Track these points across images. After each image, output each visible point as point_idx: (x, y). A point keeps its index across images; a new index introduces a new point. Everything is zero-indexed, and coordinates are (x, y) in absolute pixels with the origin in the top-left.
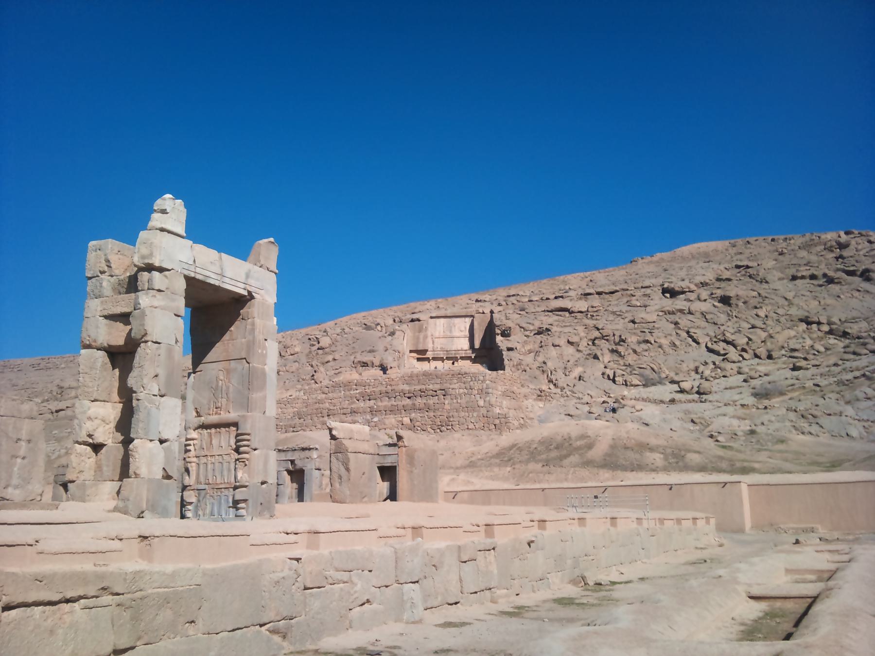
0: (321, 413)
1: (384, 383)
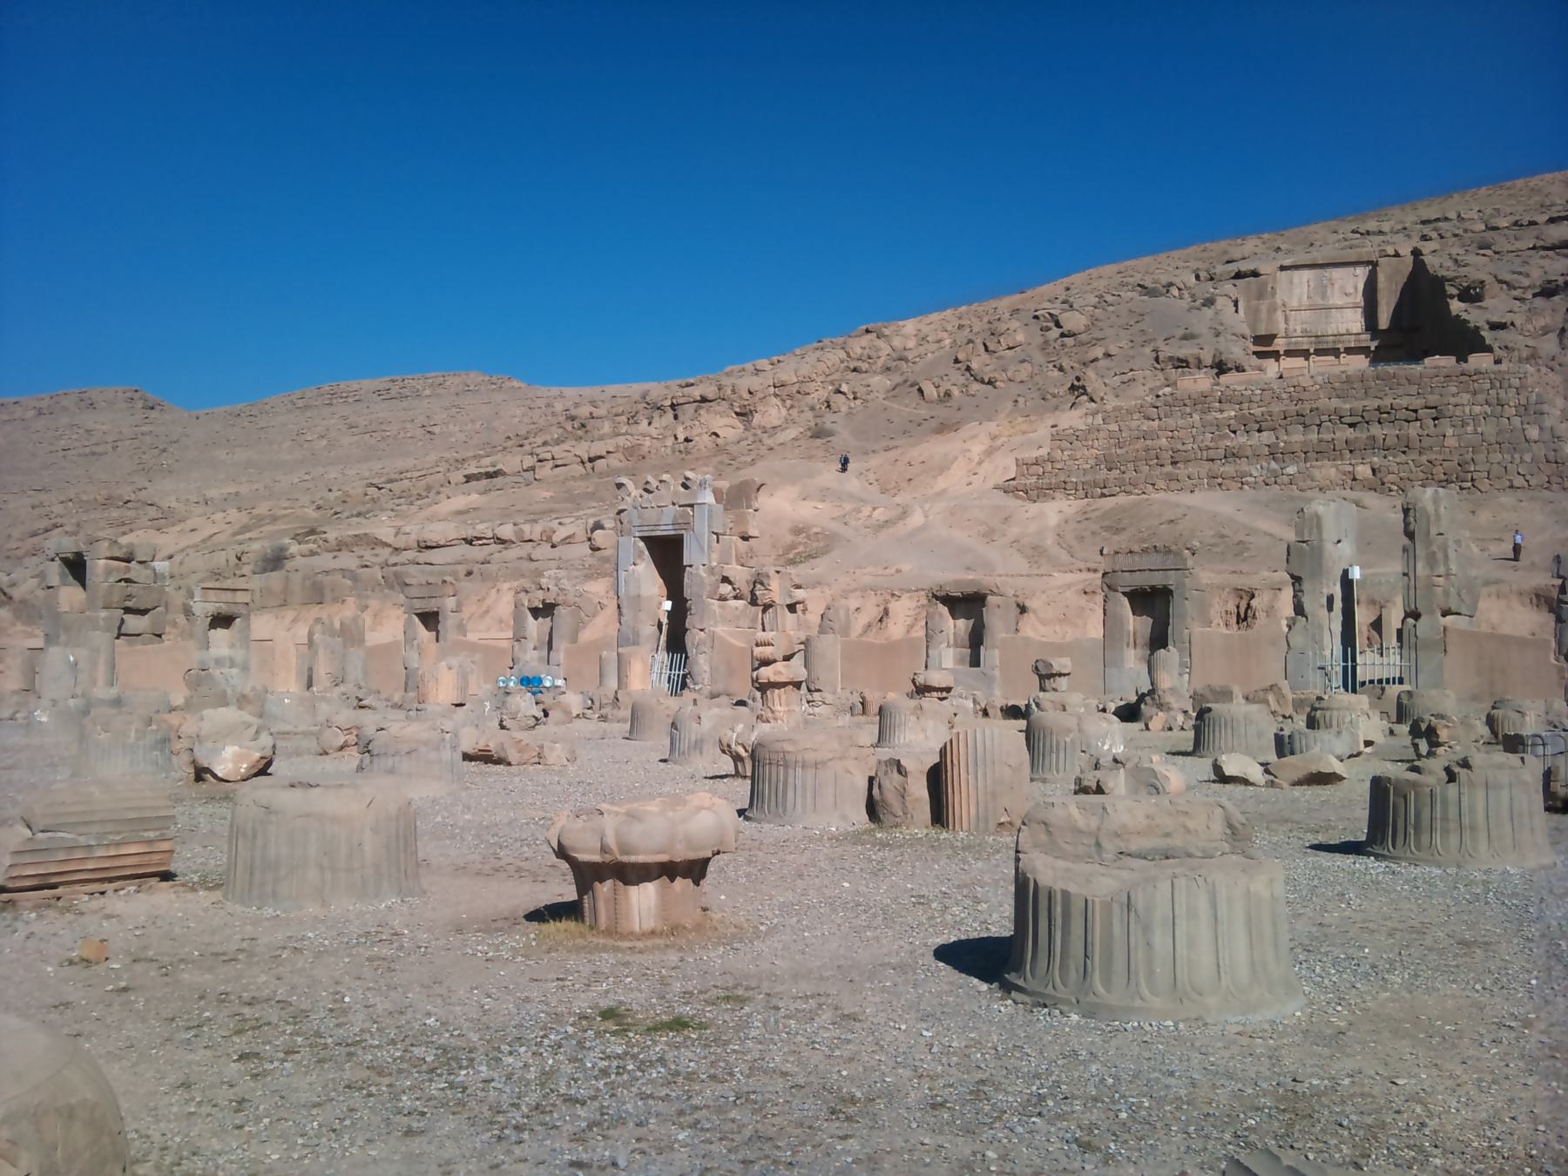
0: (1157, 458)
1: (1284, 396)
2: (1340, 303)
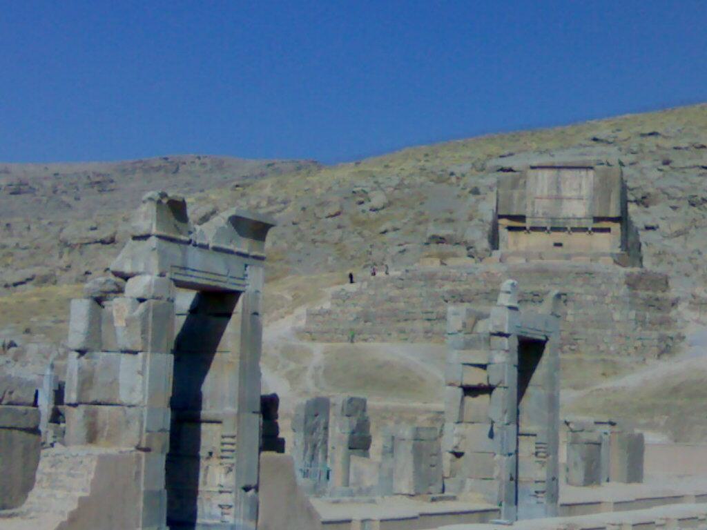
2: (569, 195)
